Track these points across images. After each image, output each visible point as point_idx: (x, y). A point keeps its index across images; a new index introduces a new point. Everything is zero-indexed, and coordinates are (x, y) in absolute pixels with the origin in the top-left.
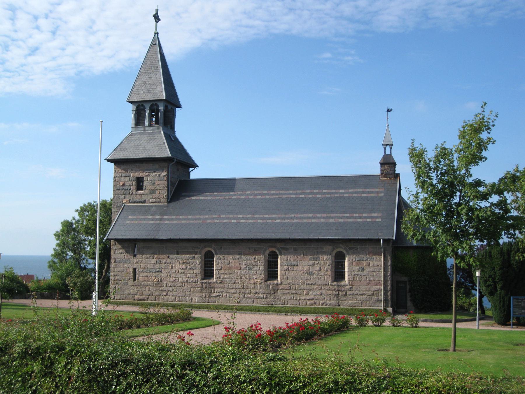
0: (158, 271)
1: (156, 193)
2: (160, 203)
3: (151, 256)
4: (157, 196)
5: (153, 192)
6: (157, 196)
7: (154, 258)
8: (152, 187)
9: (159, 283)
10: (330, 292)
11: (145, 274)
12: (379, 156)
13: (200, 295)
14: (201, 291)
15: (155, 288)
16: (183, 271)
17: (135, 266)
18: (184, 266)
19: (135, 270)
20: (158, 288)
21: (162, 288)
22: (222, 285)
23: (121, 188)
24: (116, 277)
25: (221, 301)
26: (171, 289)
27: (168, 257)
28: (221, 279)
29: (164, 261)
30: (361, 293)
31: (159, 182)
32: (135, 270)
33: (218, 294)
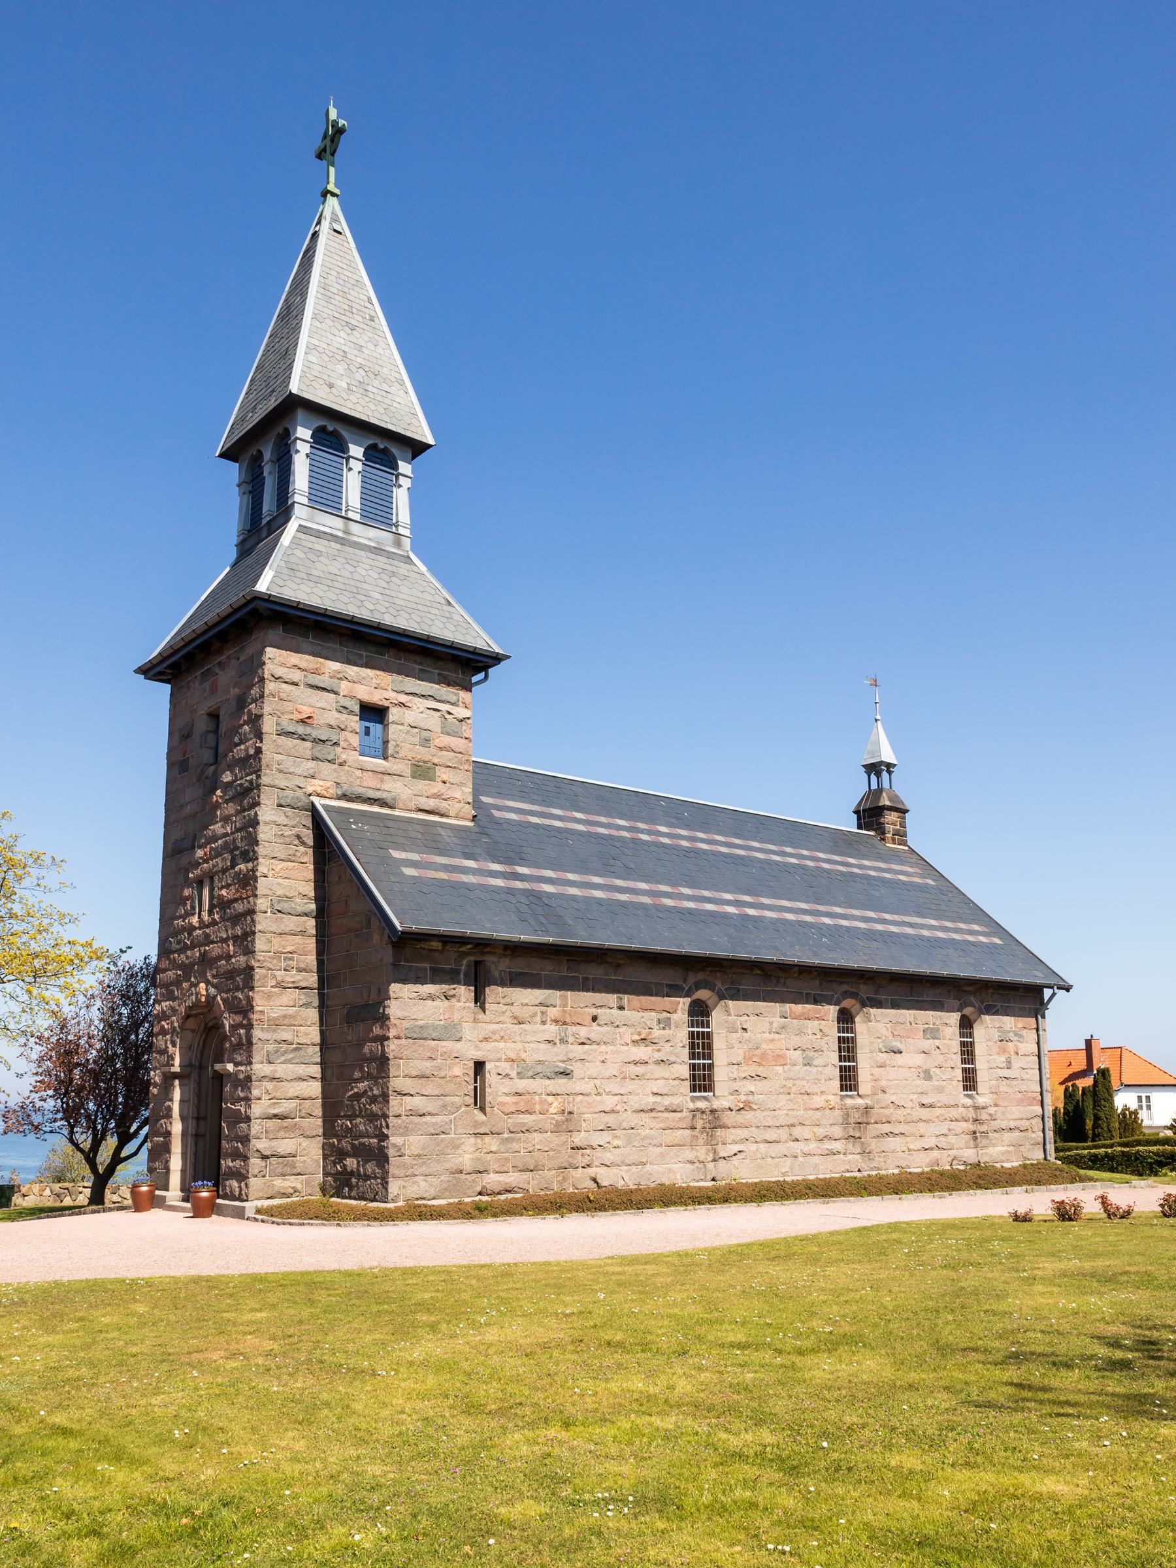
0: (565, 1074)
1: (432, 779)
2: (448, 816)
3: (535, 1015)
4: (437, 787)
5: (423, 771)
6: (437, 787)
7: (544, 1023)
8: (424, 754)
9: (567, 1122)
10: (963, 1125)
11: (522, 1085)
12: (857, 787)
13: (688, 1154)
14: (692, 1144)
15: (556, 1140)
16: (640, 1069)
17: (479, 1055)
18: (642, 1052)
19: (479, 1066)
20: (563, 1138)
21: (578, 1139)
22: (748, 1116)
23: (301, 729)
24: (407, 1099)
25: (745, 1172)
26: (604, 1138)
27: (594, 1019)
28: (743, 1098)
29: (583, 1032)
30: (1012, 1125)
31: (446, 740)
32: (479, 1066)
33: (736, 1148)
